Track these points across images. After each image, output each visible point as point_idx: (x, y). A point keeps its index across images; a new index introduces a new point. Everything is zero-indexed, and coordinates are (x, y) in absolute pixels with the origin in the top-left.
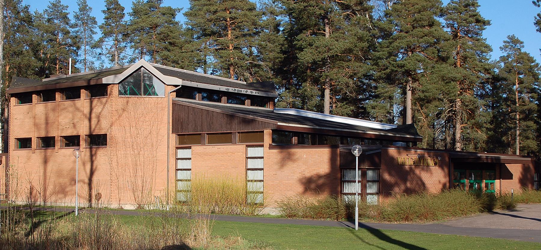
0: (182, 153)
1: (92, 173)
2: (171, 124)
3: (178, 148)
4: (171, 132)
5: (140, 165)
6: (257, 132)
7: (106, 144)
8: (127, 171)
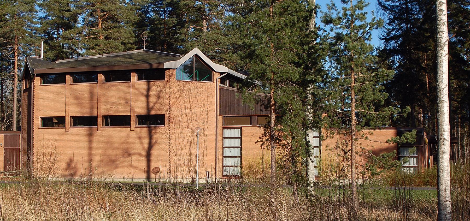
0: (227, 133)
1: (150, 147)
2: (218, 107)
3: (224, 128)
4: (218, 114)
5: (194, 143)
6: (242, 116)
7: (164, 124)
8: (184, 148)
